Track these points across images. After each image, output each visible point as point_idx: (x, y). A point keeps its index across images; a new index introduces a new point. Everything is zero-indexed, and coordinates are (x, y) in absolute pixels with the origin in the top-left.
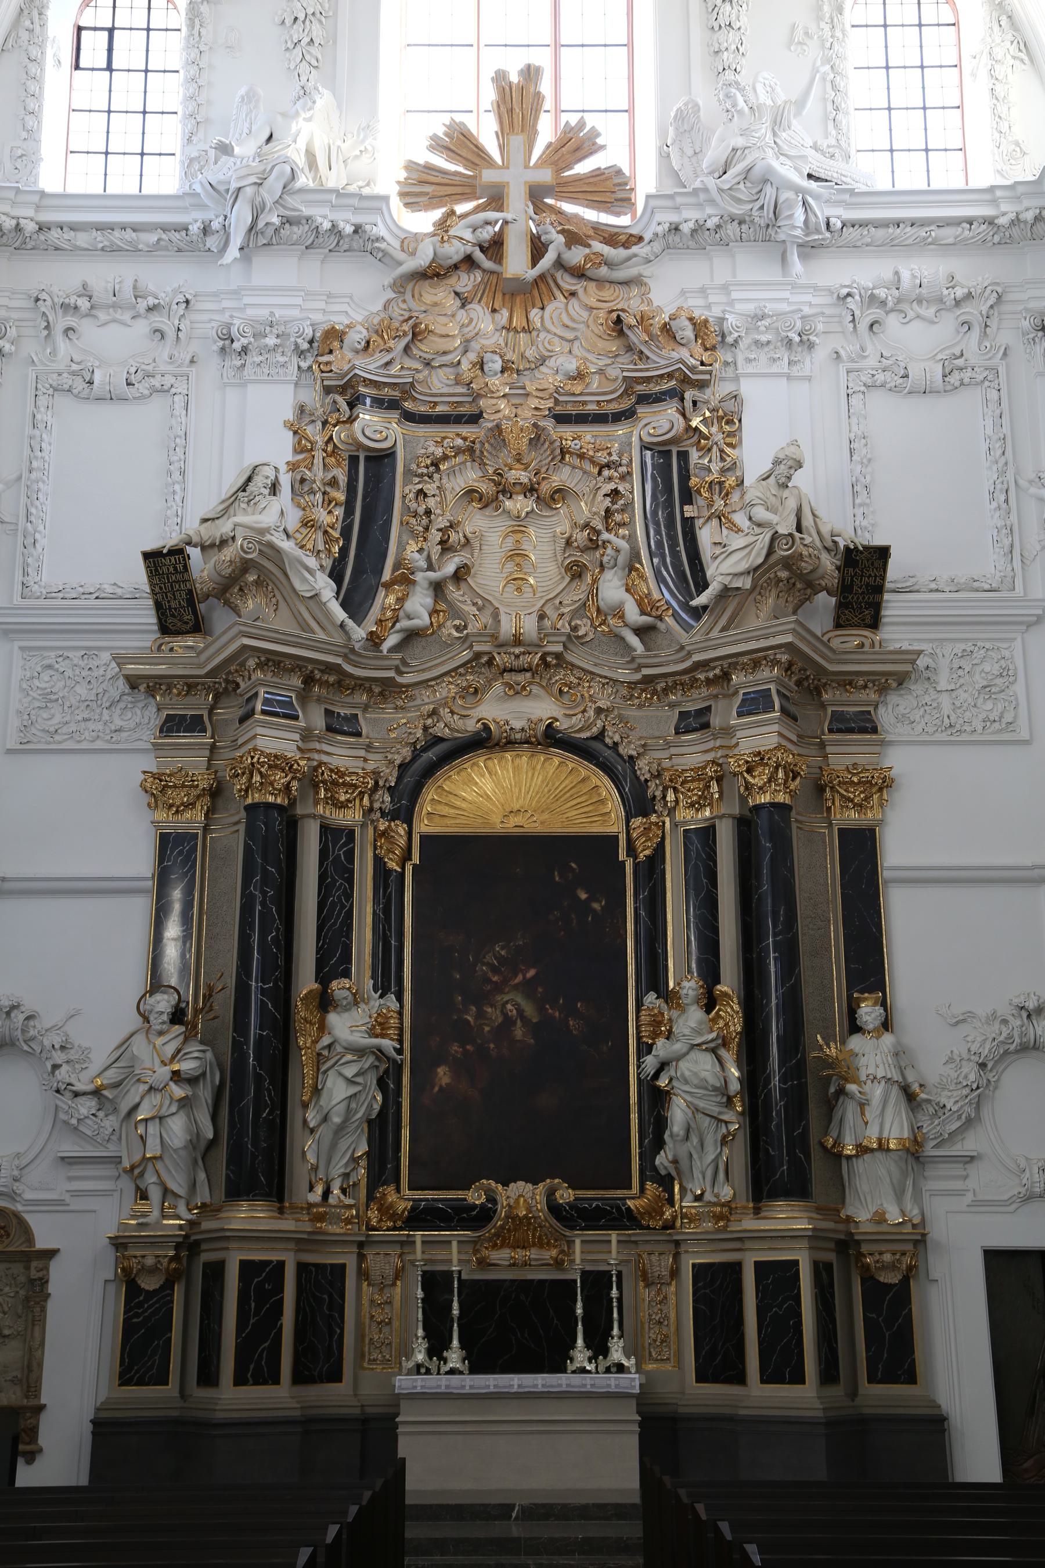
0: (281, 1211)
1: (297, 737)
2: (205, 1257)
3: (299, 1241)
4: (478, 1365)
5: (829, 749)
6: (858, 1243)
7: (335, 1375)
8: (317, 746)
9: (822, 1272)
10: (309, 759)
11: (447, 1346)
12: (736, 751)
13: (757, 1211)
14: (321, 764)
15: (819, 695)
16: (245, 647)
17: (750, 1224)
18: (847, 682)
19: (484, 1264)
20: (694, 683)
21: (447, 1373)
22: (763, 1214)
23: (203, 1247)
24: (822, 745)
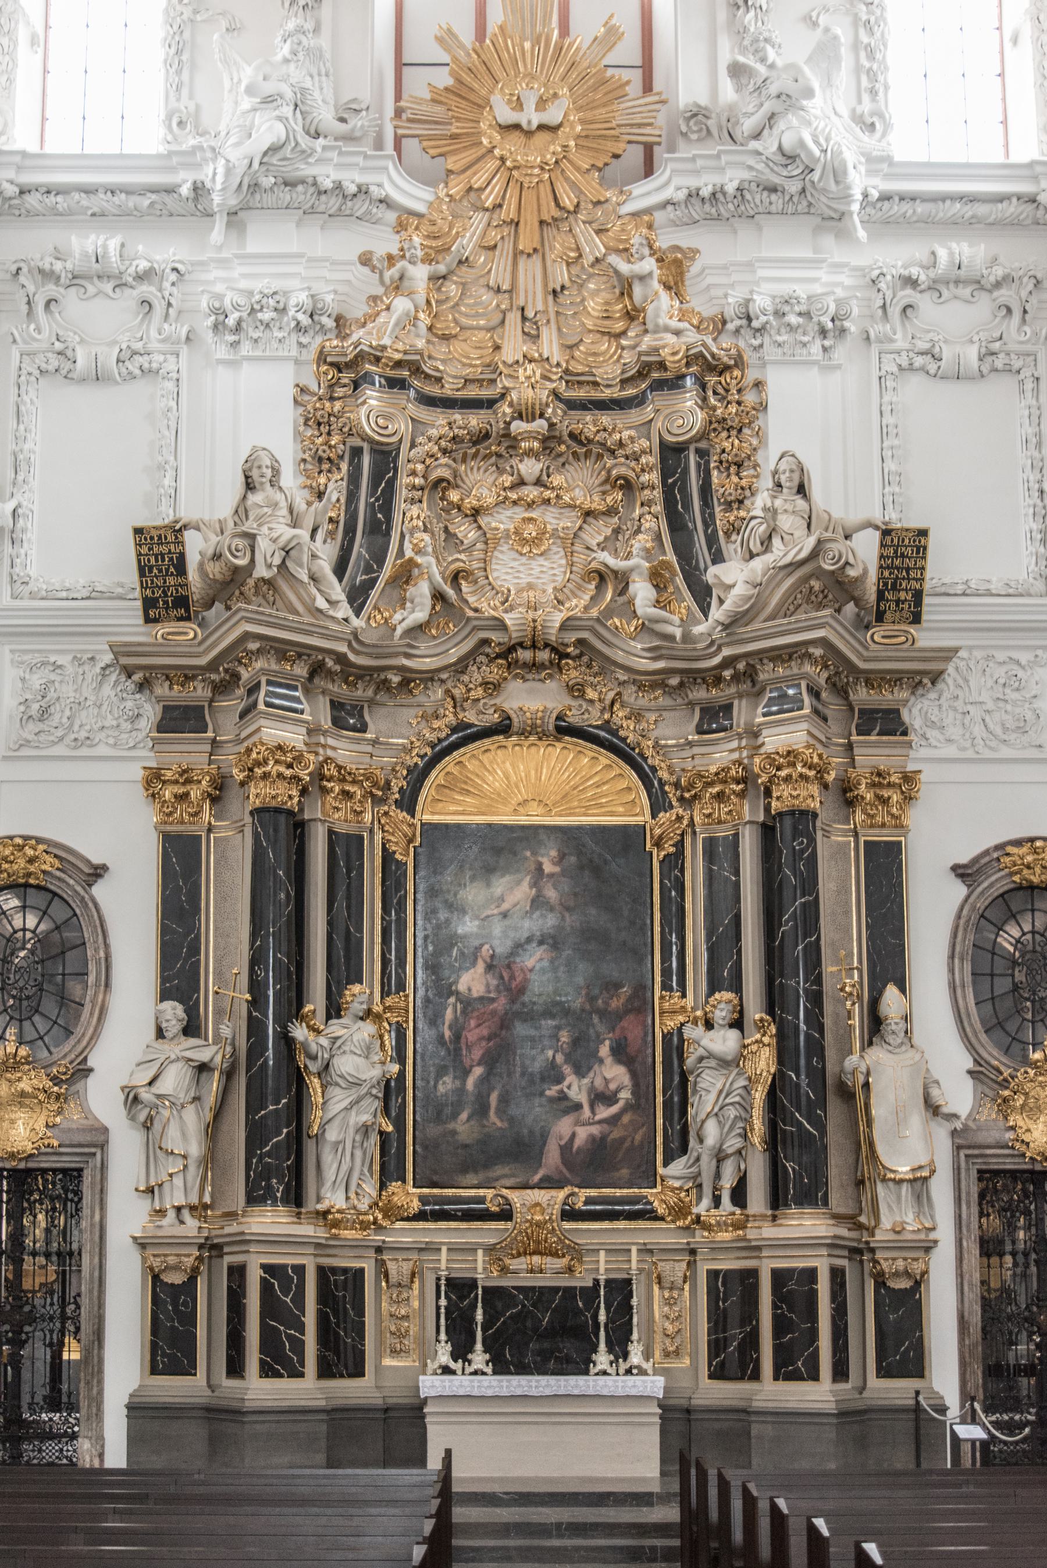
0: (298, 1215)
1: (304, 731)
2: (227, 1259)
3: (318, 1245)
4: (501, 1366)
5: (856, 751)
6: (872, 1251)
7: (358, 1372)
8: (322, 740)
9: (837, 1275)
10: (317, 754)
11: (470, 1348)
12: (762, 750)
13: (774, 1218)
14: (327, 760)
15: (846, 692)
16: (246, 636)
17: (769, 1232)
18: (873, 680)
19: (504, 1270)
20: (718, 680)
21: (471, 1374)
22: (779, 1222)
23: (226, 1249)
24: (850, 747)
